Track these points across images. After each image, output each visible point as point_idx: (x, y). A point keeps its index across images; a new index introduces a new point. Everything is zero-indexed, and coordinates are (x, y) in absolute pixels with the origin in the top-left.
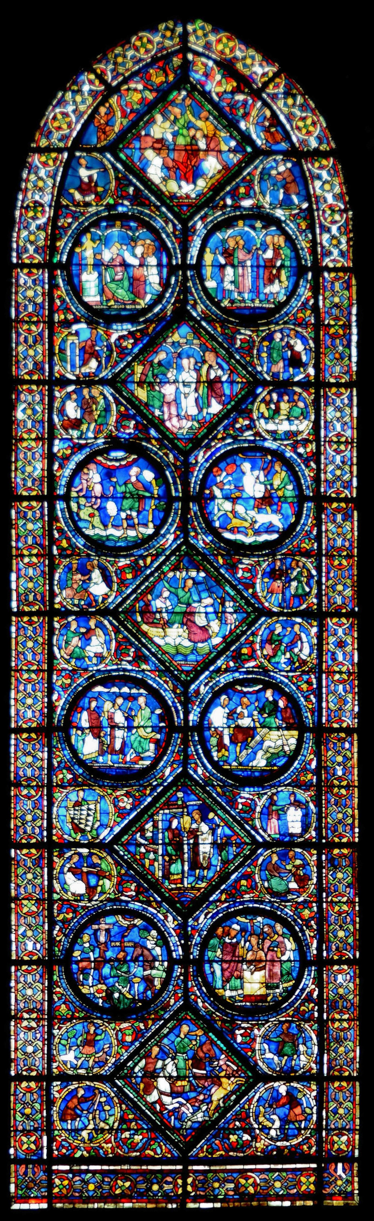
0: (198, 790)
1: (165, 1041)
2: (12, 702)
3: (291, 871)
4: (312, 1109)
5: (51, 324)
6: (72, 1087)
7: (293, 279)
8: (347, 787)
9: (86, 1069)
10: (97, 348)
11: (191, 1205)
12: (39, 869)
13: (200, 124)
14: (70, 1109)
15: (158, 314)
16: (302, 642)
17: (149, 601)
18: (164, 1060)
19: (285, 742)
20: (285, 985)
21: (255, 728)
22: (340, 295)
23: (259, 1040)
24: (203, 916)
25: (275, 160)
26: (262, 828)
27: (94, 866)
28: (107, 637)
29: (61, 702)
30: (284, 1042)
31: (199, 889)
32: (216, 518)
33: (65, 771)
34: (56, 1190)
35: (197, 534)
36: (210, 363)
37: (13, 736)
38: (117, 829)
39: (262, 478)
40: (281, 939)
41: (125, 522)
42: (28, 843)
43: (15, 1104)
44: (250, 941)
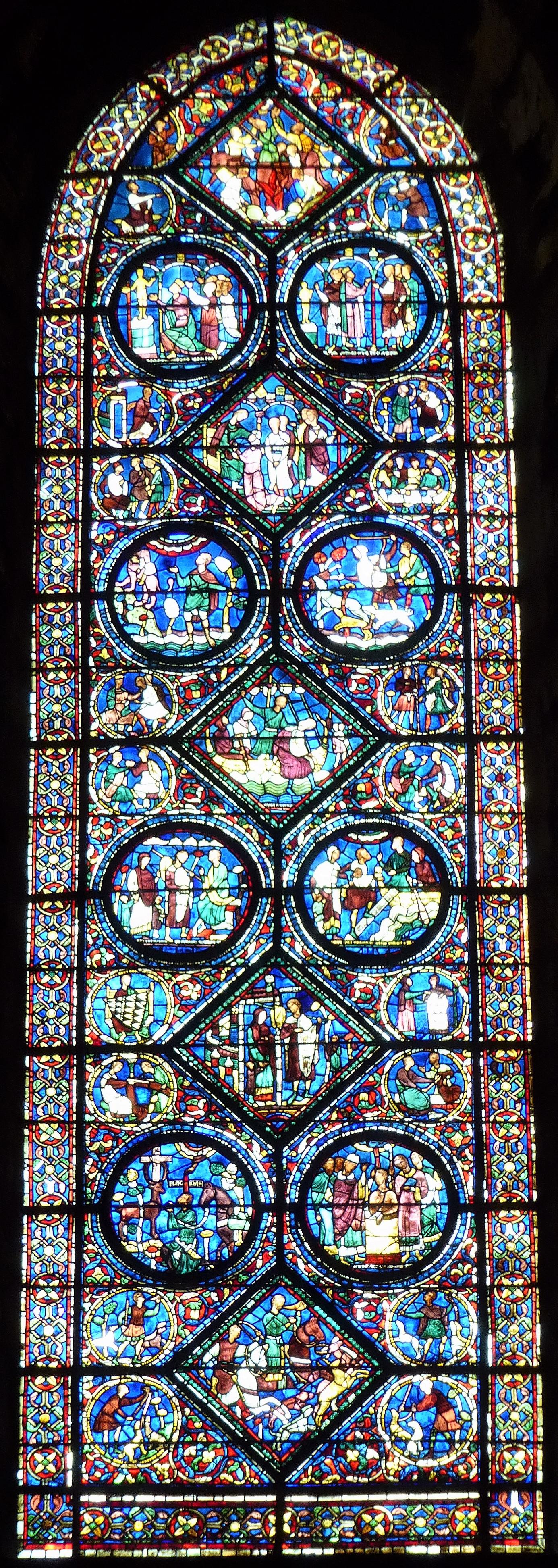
0: (296, 973)
1: (250, 1318)
2: (30, 861)
3: (433, 1079)
4: (470, 1414)
5: (87, 379)
6: (111, 1384)
7: (422, 320)
8: (515, 966)
9: (132, 1358)
10: (152, 411)
11: (287, 1551)
12: (64, 1082)
13: (292, 138)
14: (108, 1414)
15: (236, 366)
16: (444, 775)
17: (225, 726)
18: (248, 1345)
19: (422, 908)
20: (427, 1239)
21: (378, 889)
22: (487, 337)
23: (389, 1316)
24: (304, 1143)
25: (394, 177)
26: (390, 1022)
27: (145, 1076)
28: (165, 773)
29: (98, 860)
30: (427, 1318)
31: (298, 1108)
32: (318, 617)
33: (103, 950)
34: (85, 1531)
35: (292, 638)
36: (308, 422)
37: (30, 905)
38: (178, 1027)
39: (383, 564)
40: (420, 1175)
41: (190, 625)
42: (50, 1046)
43: (26, 1407)
44: (374, 1178)
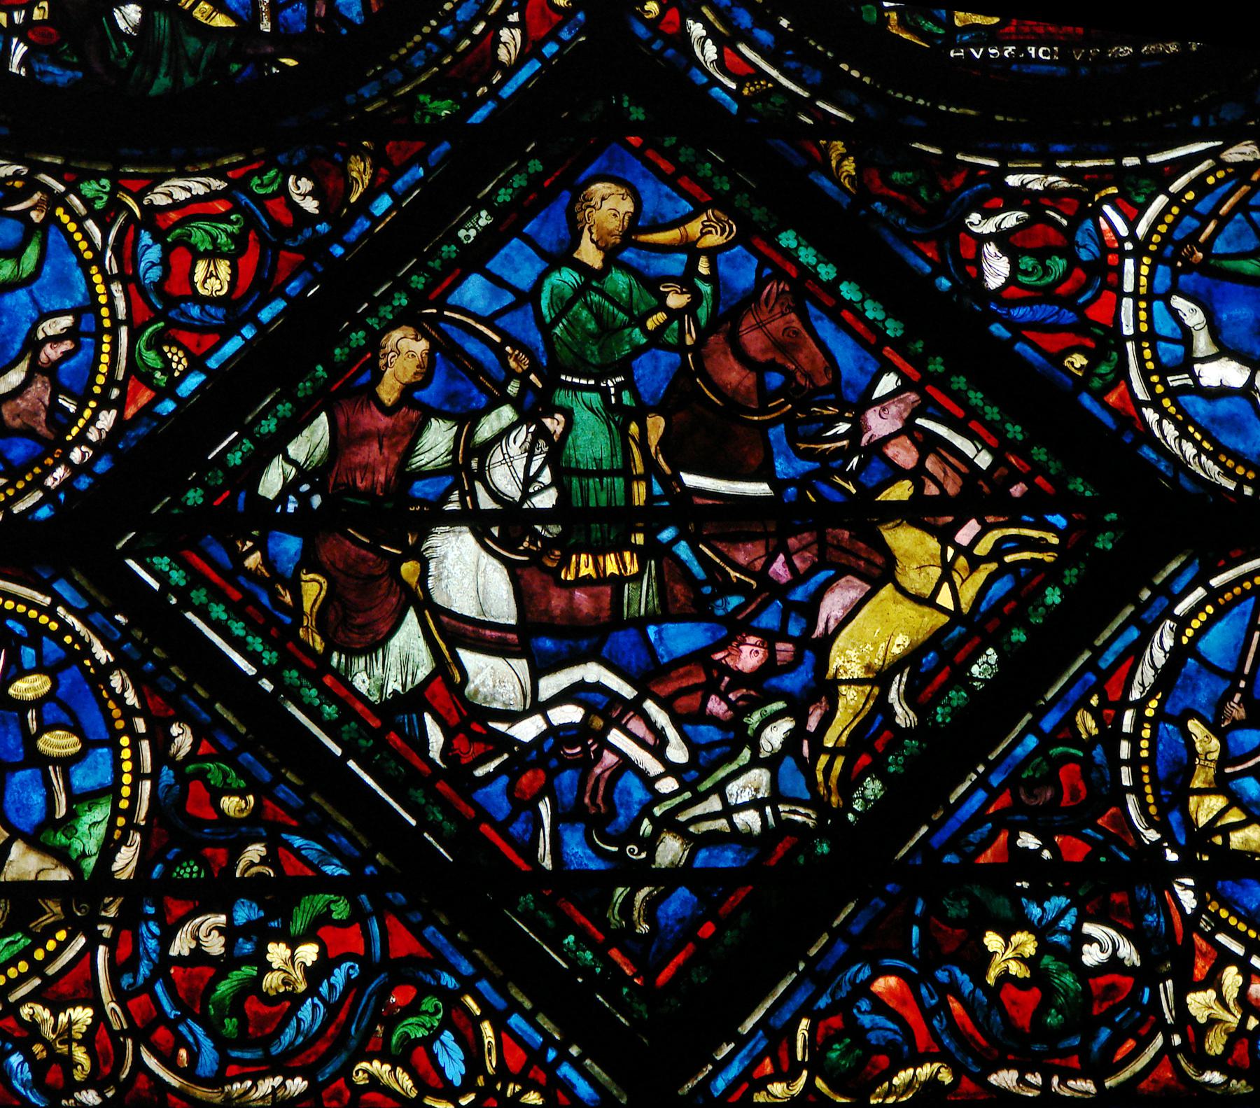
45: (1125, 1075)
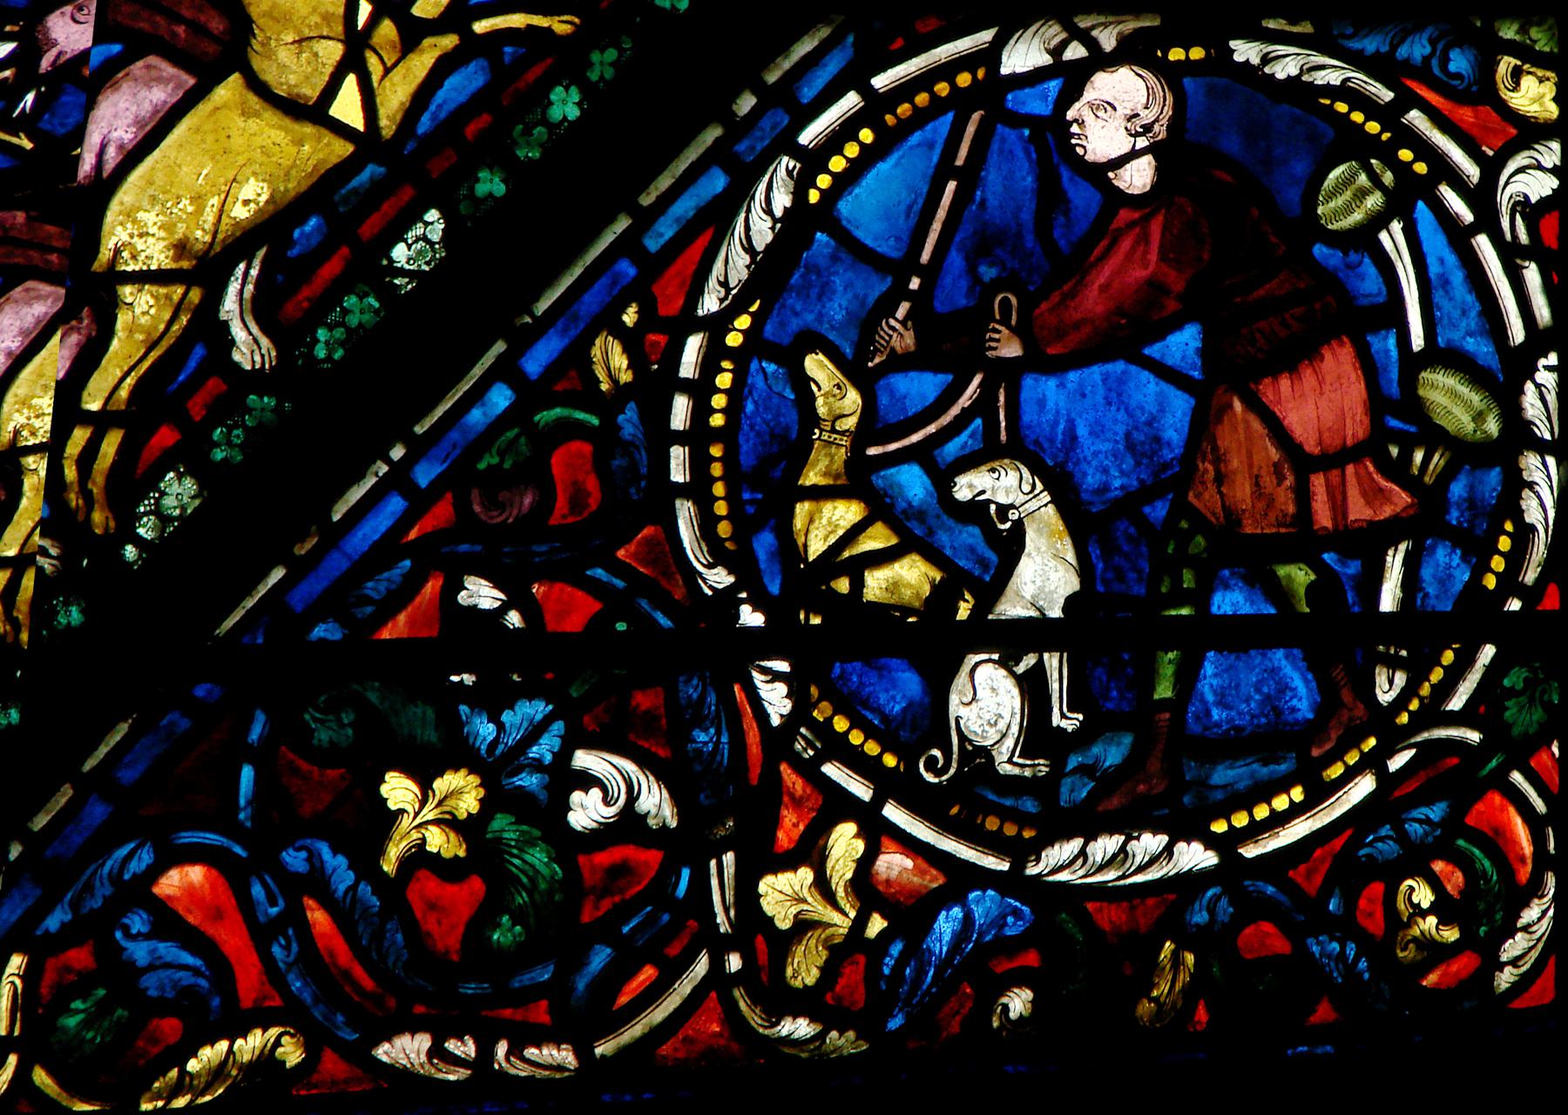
4: (1502, 381)
45: (635, 1030)
